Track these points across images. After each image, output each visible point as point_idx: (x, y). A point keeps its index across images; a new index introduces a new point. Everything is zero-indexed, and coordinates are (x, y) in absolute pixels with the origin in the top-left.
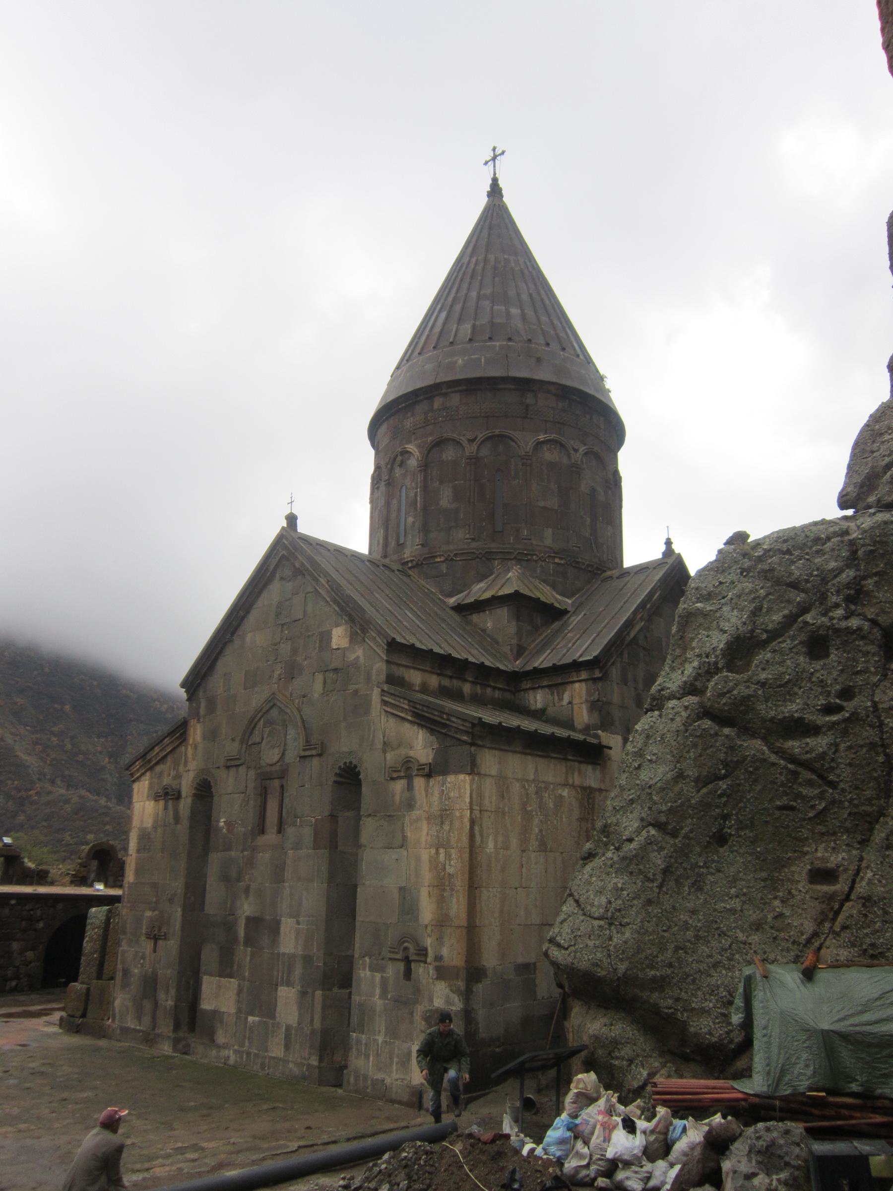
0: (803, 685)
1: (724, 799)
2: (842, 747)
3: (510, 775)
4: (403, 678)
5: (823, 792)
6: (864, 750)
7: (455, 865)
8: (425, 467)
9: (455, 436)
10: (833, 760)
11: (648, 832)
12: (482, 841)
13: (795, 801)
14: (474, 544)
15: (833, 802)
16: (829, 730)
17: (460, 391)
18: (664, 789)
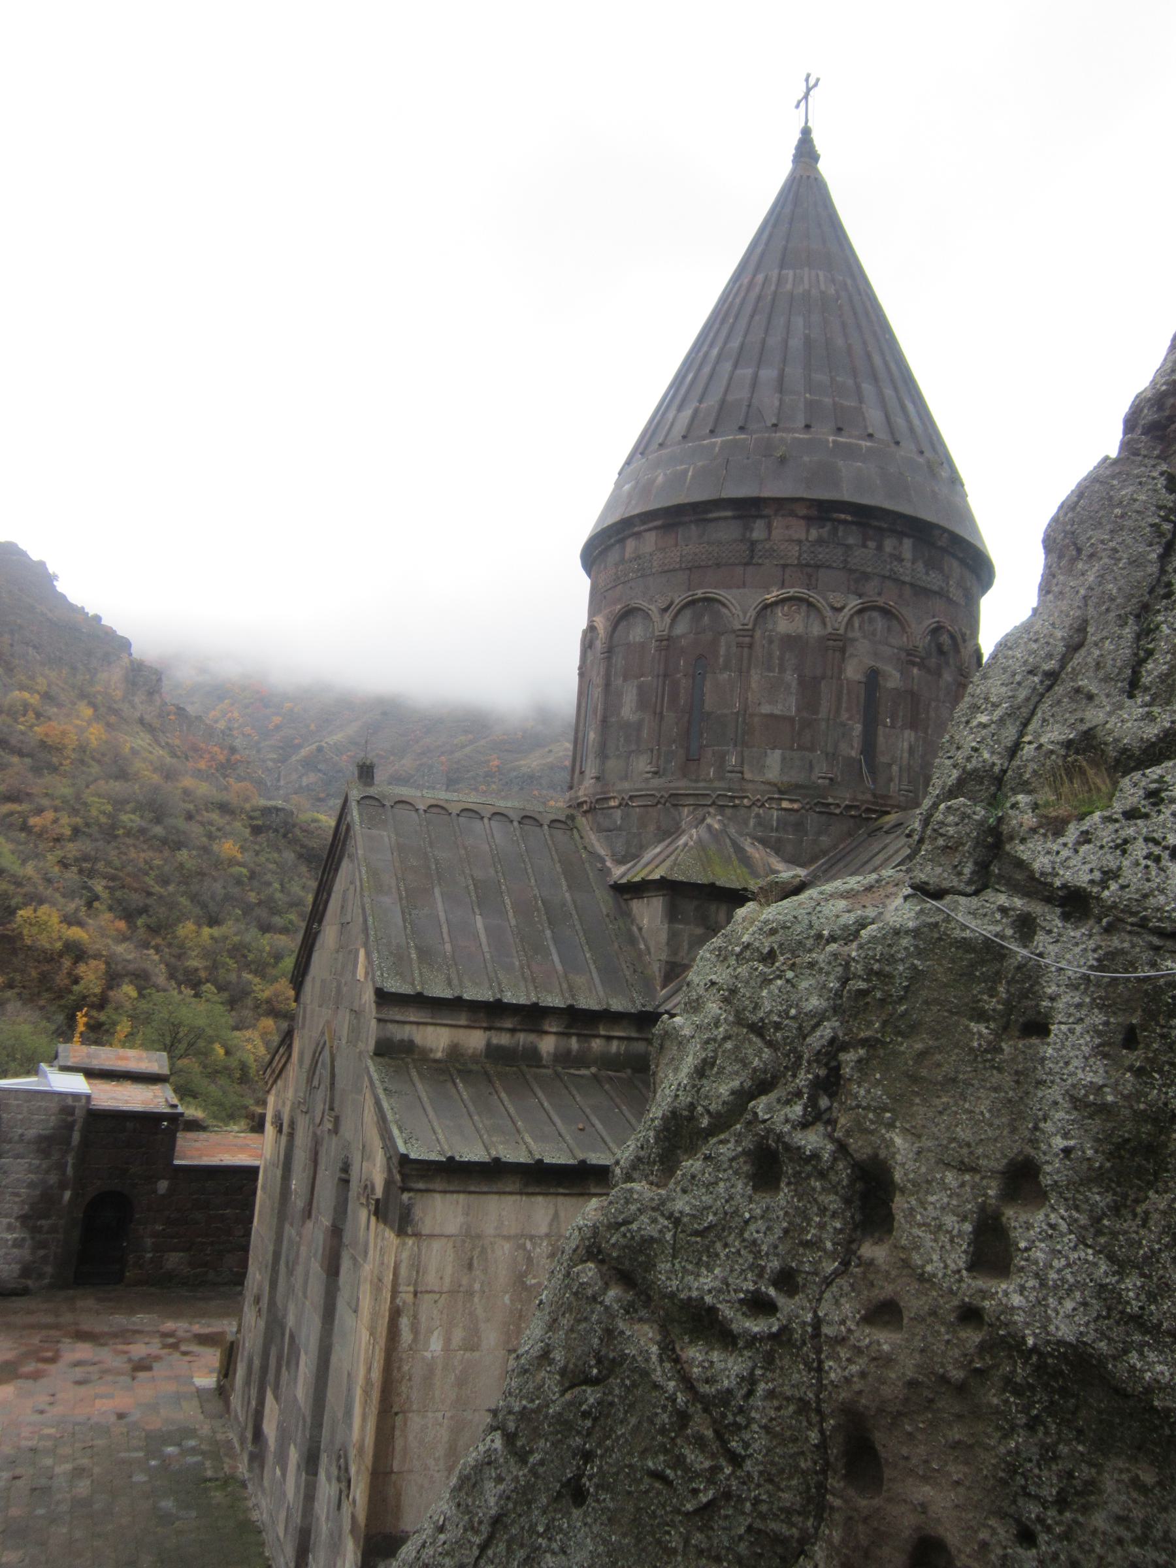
0: (730, 1239)
1: (588, 1423)
2: (761, 1388)
3: (489, 1229)
4: (411, 1042)
5: (716, 1469)
6: (792, 1408)
7: (376, 1375)
8: (609, 651)
9: (645, 605)
10: (741, 1410)
11: (493, 1441)
12: (415, 1340)
13: (674, 1468)
14: (656, 782)
15: (727, 1495)
16: (745, 1348)
17: (656, 528)
18: (526, 1371)
